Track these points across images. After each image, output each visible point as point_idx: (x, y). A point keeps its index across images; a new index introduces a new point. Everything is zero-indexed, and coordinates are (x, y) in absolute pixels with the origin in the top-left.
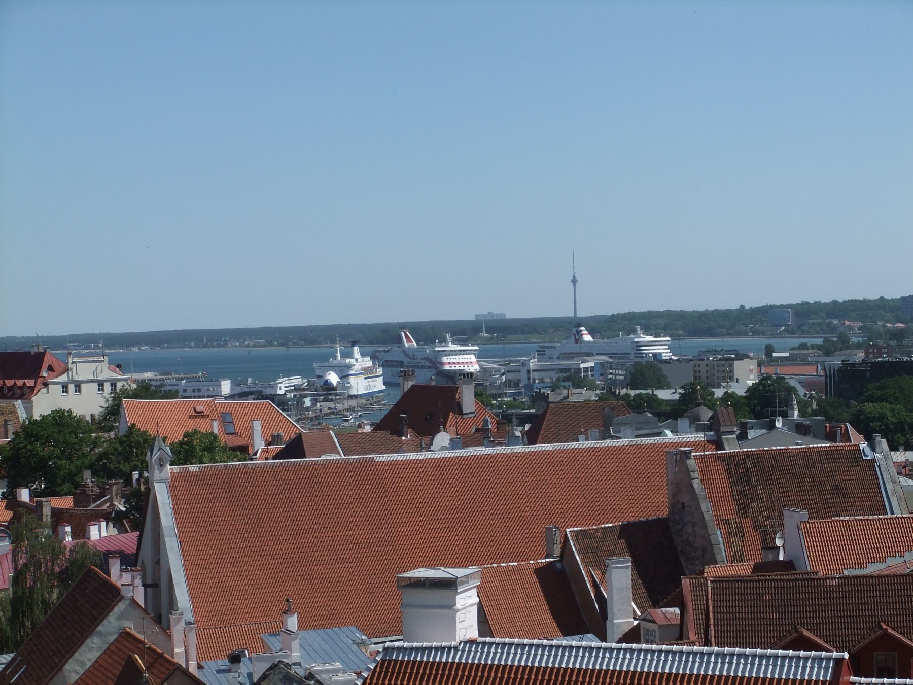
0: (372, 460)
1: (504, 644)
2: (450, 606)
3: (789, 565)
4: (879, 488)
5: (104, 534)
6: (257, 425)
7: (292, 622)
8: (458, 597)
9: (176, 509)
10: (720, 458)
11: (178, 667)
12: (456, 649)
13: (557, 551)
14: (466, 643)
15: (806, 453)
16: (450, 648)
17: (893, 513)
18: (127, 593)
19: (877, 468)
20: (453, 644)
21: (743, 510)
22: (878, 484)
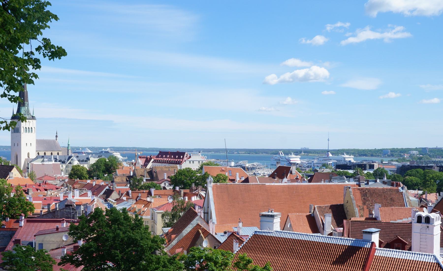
0: (265, 184)
1: (285, 232)
2: (272, 222)
3: (375, 219)
4: (404, 200)
5: (196, 199)
6: (238, 174)
7: (241, 224)
8: (274, 220)
9: (214, 194)
10: (359, 189)
11: (210, 234)
12: (273, 233)
13: (312, 211)
14: (275, 231)
15: (383, 189)
16: (271, 232)
17: (407, 207)
18: (199, 214)
19: (403, 195)
20: (272, 231)
21: (364, 203)
22: (403, 199)
